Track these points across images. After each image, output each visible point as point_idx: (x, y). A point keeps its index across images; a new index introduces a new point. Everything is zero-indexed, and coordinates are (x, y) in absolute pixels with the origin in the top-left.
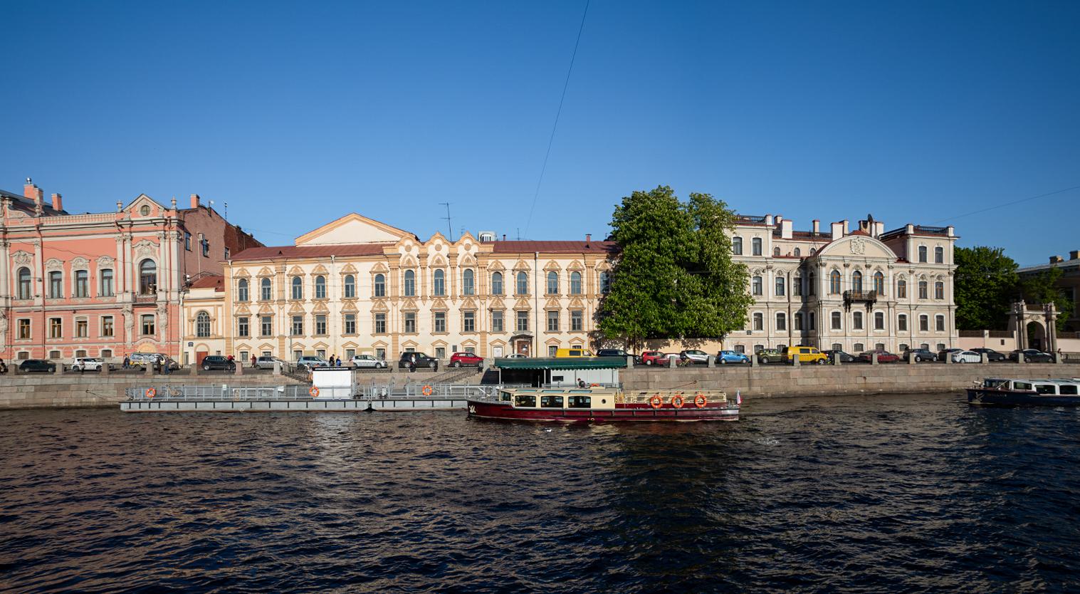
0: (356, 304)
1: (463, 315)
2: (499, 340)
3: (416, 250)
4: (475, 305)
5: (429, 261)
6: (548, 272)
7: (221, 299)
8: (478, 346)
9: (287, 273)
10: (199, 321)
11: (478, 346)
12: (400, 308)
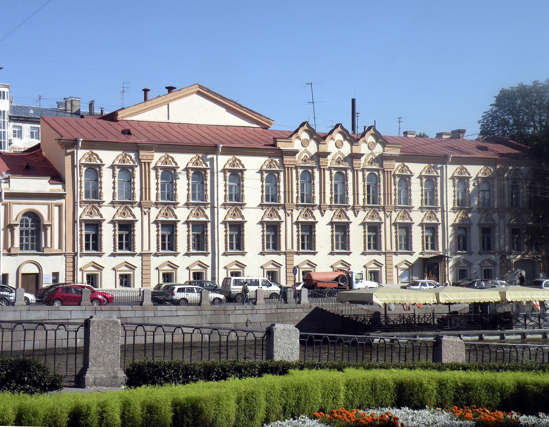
0: (244, 212)
1: (117, 228)
2: (407, 263)
3: (312, 148)
4: (380, 219)
5: (329, 161)
6: (265, 175)
7: (61, 196)
8: (383, 268)
9: (152, 165)
10: (22, 226)
11: (383, 268)
12: (295, 220)
